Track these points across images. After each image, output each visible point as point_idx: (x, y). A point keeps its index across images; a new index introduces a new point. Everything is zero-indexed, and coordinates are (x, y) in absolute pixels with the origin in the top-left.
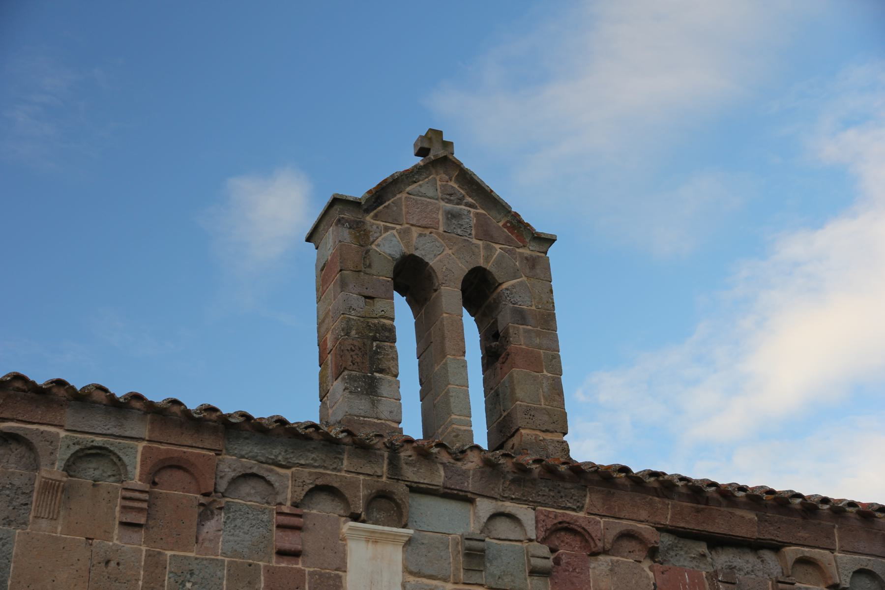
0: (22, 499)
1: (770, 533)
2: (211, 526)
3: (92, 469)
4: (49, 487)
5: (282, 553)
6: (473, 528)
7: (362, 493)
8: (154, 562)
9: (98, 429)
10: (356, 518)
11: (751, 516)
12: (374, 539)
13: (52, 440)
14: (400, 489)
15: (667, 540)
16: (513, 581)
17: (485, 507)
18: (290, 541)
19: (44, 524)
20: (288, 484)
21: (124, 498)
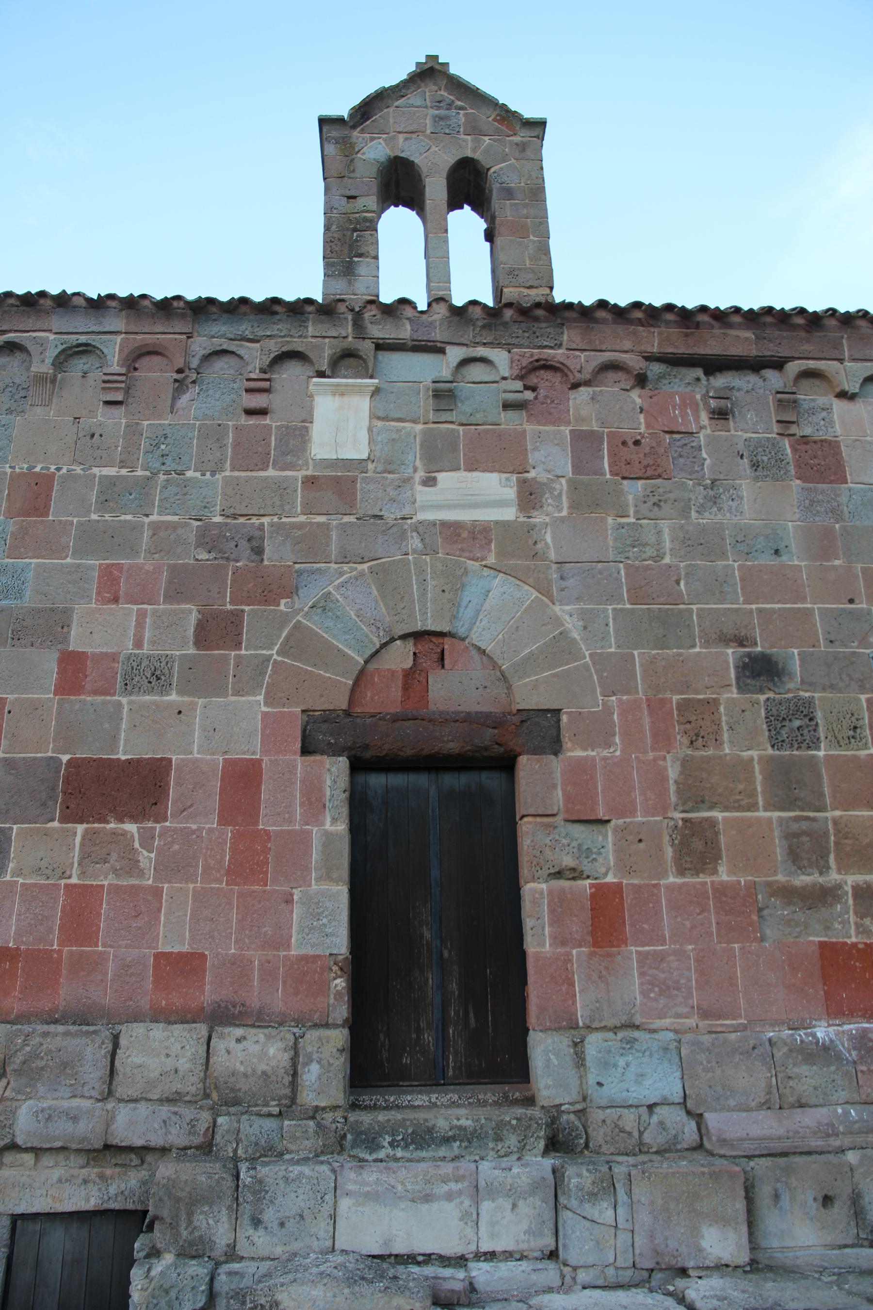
0: (23, 393)
1: (770, 350)
2: (185, 398)
3: (80, 364)
4: (40, 379)
5: (249, 412)
6: (446, 373)
7: (327, 353)
8: (133, 430)
9: (80, 328)
10: (321, 374)
11: (749, 334)
12: (340, 391)
13: (42, 343)
14: (366, 347)
15: (656, 368)
16: (485, 416)
17: (455, 354)
18: (258, 401)
19: (39, 410)
20: (255, 356)
21: (104, 382)
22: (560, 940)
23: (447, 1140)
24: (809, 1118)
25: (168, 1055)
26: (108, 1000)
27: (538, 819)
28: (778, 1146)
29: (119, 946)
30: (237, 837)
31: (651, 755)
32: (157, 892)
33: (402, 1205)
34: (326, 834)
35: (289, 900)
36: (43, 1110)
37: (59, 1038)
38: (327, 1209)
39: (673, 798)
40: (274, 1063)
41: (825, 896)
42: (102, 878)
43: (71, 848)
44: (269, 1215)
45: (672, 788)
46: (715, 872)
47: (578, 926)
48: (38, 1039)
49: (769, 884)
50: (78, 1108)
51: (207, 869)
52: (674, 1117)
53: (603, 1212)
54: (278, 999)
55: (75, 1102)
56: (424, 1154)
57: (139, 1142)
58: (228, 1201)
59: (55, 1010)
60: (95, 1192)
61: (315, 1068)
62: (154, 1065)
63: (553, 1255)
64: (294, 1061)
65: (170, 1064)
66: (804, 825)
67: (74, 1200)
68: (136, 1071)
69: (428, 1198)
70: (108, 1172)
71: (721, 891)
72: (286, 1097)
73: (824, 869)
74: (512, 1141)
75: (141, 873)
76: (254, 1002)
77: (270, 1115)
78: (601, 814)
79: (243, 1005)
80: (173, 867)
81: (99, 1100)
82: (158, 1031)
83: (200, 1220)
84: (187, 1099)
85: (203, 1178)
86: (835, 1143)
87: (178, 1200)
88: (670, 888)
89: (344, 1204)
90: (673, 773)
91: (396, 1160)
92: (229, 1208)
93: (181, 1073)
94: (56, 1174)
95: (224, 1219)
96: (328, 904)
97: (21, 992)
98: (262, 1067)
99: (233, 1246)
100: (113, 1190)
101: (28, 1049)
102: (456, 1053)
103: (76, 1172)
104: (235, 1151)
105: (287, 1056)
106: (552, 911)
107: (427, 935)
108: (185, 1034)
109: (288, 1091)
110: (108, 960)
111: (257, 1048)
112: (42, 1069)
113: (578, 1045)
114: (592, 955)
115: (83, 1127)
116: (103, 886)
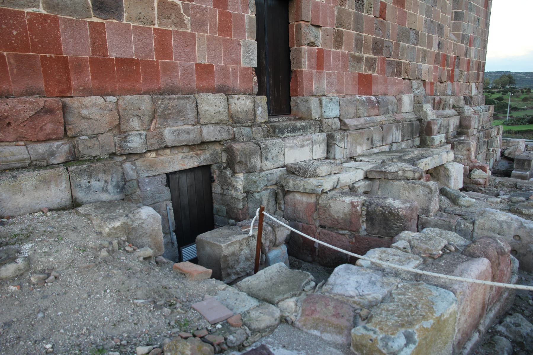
22: (310, 67)
23: (300, 129)
24: (362, 120)
25: (216, 106)
26: (180, 84)
27: (305, 23)
28: (359, 127)
29: (181, 60)
30: (221, 14)
31: (332, 5)
32: (193, 36)
33: (298, 149)
34: (250, 17)
35: (239, 45)
36: (175, 131)
37: (176, 100)
38: (283, 152)
39: (335, 22)
40: (249, 107)
41: (359, 59)
42: (169, 26)
43: (153, 9)
44: (270, 156)
45: (335, 18)
46: (342, 49)
47: (314, 62)
48: (167, 101)
49: (351, 54)
50: (188, 129)
51: (211, 27)
52: (337, 120)
53: (342, 145)
54: (238, 84)
55: (186, 127)
56: (295, 134)
57: (213, 139)
58: (259, 153)
59: (159, 89)
60: (196, 160)
61: (260, 108)
62: (212, 110)
63: (327, 158)
64: (254, 106)
65: (217, 109)
66: (359, 37)
67: (189, 164)
68: (206, 113)
69: (303, 146)
70: (199, 152)
71: (343, 54)
72: (253, 119)
73: (361, 52)
74: (313, 129)
75: (186, 26)
76: (231, 85)
77: (248, 126)
78: (320, 24)
79: (228, 86)
80: (198, 25)
81: (194, 125)
82: (211, 96)
83: (253, 160)
84: (224, 122)
85: (251, 146)
86: (367, 126)
87: (246, 155)
88: (333, 52)
89: (286, 150)
90: (336, 13)
91: (289, 136)
92: (260, 155)
93: (221, 113)
94: (180, 156)
95: (259, 159)
96: (251, 47)
97: (143, 81)
98: (246, 109)
99: (261, 167)
100: (202, 158)
101: (163, 105)
102: (272, 105)
103: (187, 154)
104: (243, 139)
105: (252, 105)
106: (308, 56)
107: (264, 62)
108: (220, 97)
109: (253, 117)
110: (178, 66)
111: (243, 102)
112: (170, 114)
113: (320, 101)
114: (317, 72)
115: (192, 136)
116: (171, 31)
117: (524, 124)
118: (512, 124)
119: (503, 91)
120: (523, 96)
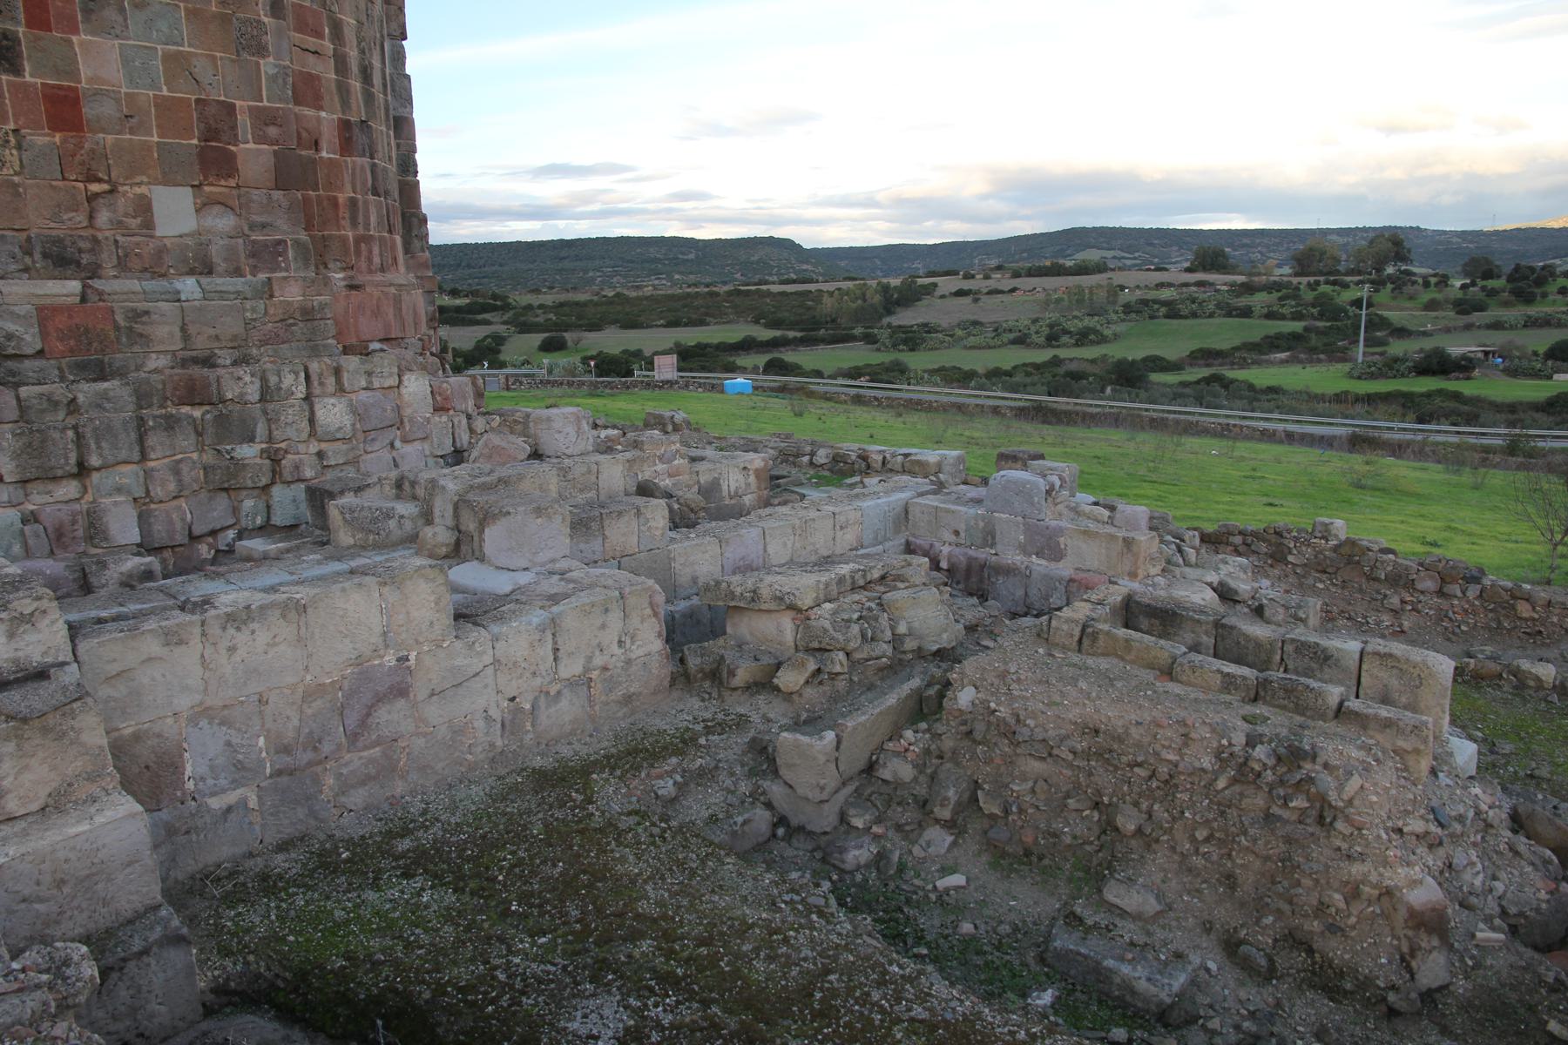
117: (1403, 376)
118: (1372, 376)
119: (1372, 282)
120: (1426, 297)
